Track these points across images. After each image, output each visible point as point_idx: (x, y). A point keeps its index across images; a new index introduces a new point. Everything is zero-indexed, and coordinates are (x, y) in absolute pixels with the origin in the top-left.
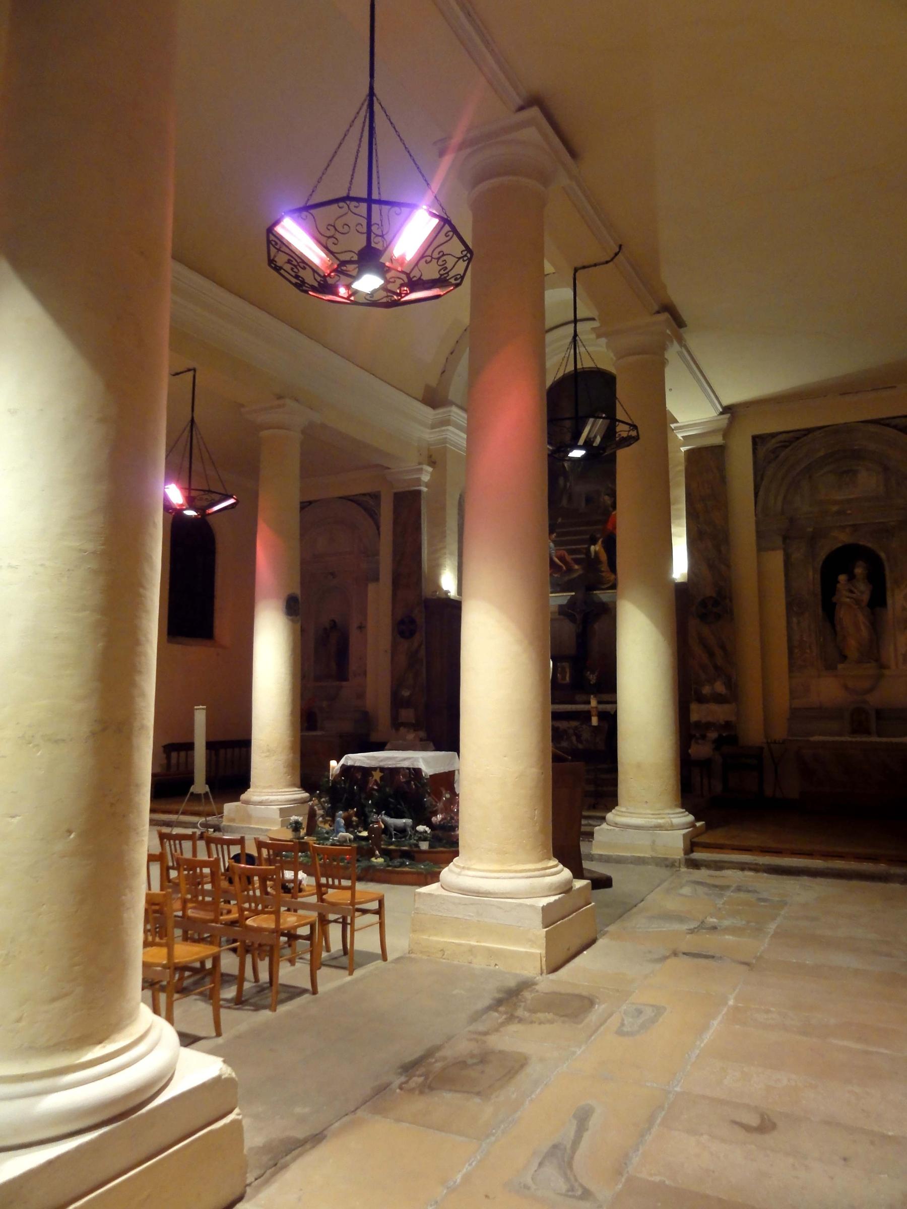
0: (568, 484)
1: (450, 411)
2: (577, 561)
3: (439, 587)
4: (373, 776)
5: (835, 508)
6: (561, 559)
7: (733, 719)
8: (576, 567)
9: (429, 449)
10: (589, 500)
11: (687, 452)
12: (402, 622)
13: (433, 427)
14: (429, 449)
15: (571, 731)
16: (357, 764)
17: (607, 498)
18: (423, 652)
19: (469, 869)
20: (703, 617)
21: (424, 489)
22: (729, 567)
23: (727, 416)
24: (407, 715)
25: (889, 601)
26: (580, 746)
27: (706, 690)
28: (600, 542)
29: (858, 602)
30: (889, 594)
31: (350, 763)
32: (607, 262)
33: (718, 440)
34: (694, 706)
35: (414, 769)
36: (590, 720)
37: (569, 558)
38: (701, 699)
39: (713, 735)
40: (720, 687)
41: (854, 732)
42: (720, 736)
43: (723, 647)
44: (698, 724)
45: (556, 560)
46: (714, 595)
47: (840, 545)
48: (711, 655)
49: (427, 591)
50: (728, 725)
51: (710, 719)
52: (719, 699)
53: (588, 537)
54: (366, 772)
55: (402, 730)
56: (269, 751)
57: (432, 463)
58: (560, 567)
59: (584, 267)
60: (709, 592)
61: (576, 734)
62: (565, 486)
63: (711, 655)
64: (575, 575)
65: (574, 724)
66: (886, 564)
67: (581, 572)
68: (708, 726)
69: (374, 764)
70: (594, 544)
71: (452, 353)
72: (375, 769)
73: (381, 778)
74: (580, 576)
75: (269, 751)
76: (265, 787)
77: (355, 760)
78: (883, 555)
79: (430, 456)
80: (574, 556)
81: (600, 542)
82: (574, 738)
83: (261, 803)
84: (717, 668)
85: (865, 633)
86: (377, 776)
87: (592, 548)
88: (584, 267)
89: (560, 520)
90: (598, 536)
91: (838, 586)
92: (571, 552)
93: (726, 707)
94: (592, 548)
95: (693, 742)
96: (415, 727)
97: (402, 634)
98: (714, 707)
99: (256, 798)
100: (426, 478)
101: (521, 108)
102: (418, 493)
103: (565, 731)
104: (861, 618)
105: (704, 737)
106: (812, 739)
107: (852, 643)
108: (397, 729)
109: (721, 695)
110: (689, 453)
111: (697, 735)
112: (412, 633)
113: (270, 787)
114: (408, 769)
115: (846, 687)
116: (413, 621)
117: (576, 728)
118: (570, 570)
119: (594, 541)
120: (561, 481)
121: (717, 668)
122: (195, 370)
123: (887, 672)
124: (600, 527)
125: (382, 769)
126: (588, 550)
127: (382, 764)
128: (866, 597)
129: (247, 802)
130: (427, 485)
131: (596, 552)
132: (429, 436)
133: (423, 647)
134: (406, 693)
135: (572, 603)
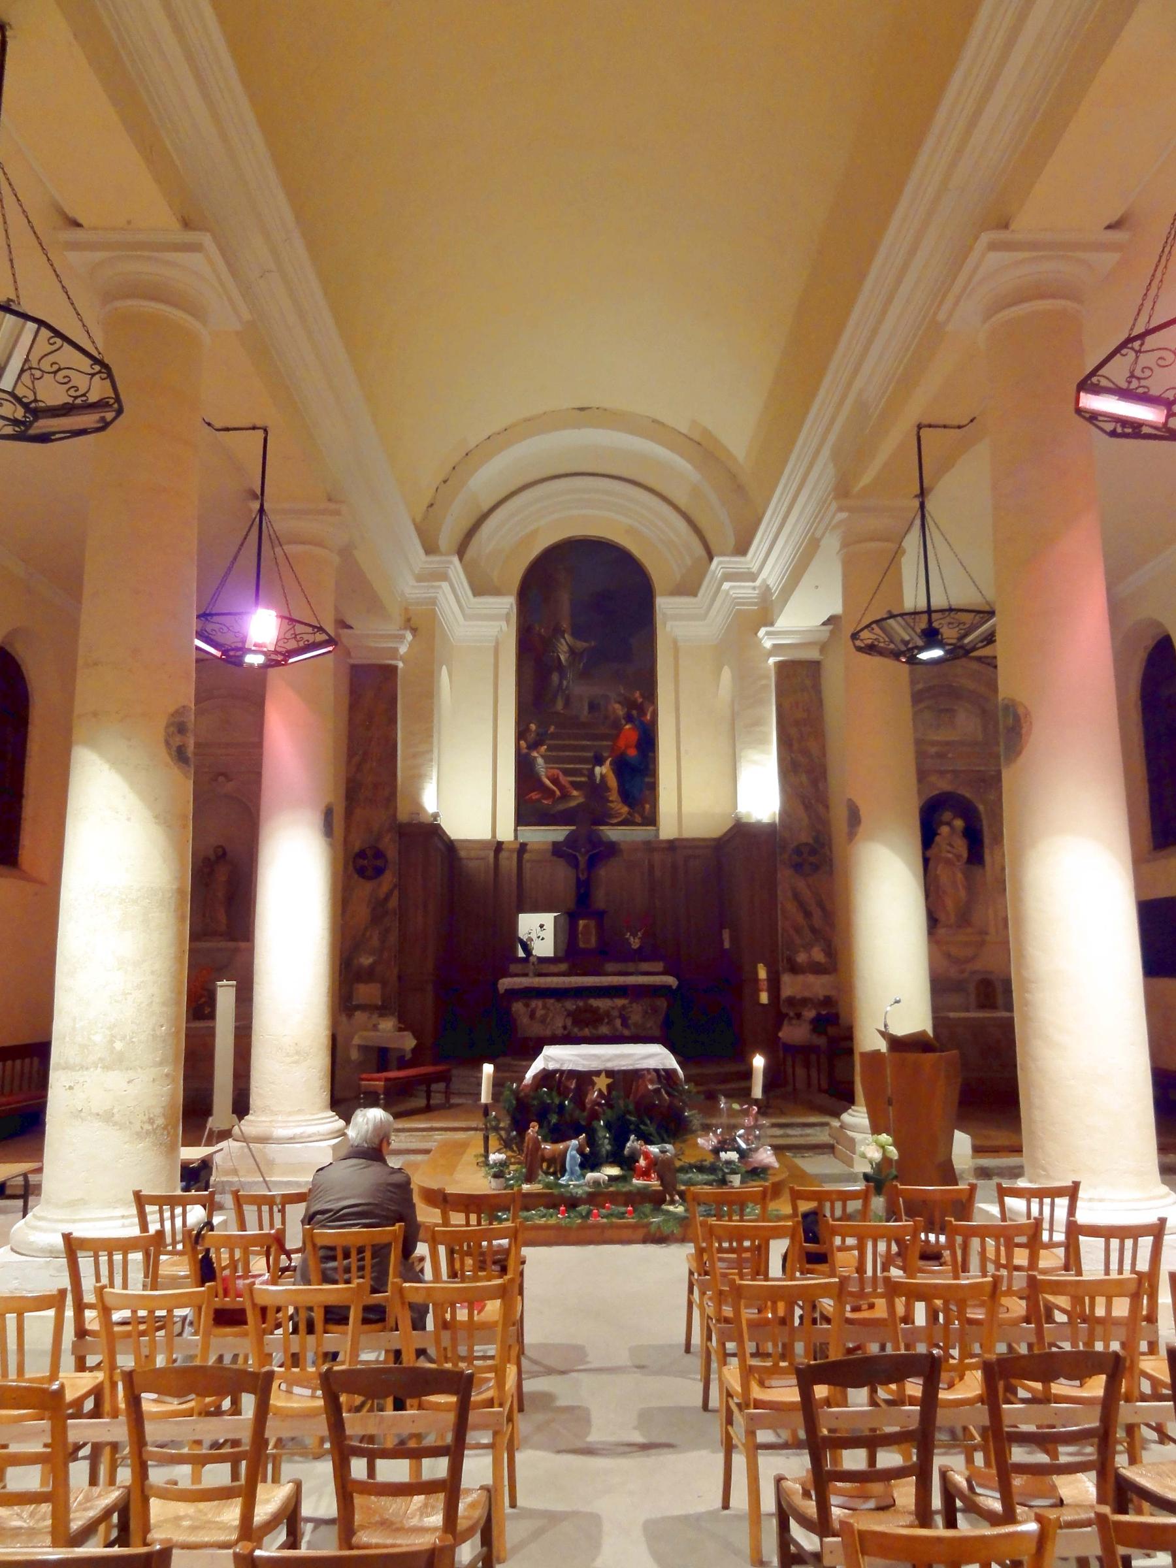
0: (565, 683)
1: (451, 562)
2: (575, 785)
3: (418, 807)
4: (593, 1084)
5: (933, 750)
6: (555, 781)
7: (833, 993)
8: (575, 793)
9: (406, 609)
10: (593, 707)
11: (776, 663)
12: (362, 854)
13: (420, 578)
14: (406, 609)
15: (615, 1013)
16: (567, 1067)
17: (617, 706)
18: (393, 903)
19: (1101, 1200)
20: (798, 867)
21: (401, 665)
22: (827, 807)
23: (830, 627)
24: (368, 992)
25: (987, 858)
27: (801, 958)
28: (608, 762)
29: (959, 857)
30: (987, 852)
31: (551, 1066)
32: (959, 427)
33: (813, 654)
34: (786, 978)
35: (666, 1071)
36: (758, 996)
37: (564, 780)
38: (795, 969)
39: (810, 1014)
40: (818, 955)
41: (982, 1006)
42: (819, 1015)
43: (821, 905)
44: (791, 1001)
45: (547, 782)
46: (811, 841)
47: (937, 792)
48: (808, 915)
49: (403, 815)
50: (828, 1001)
51: (807, 994)
52: (818, 969)
53: (591, 754)
54: (584, 1078)
55: (358, 1015)
56: (298, 1053)
57: (414, 631)
58: (554, 792)
59: (930, 426)
60: (805, 837)
62: (561, 683)
63: (808, 915)
64: (573, 804)
65: (620, 1002)
66: (983, 816)
67: (581, 800)
68: (805, 1002)
69: (594, 1065)
70: (601, 765)
71: (445, 482)
72: (598, 1073)
73: (609, 1086)
74: (579, 805)
75: (298, 1053)
76: (290, 1114)
77: (563, 1062)
78: (981, 808)
79: (409, 620)
80: (571, 779)
81: (608, 762)
82: (618, 1022)
83: (291, 1140)
84: (813, 930)
85: (963, 894)
86: (602, 1083)
87: (598, 770)
88: (930, 426)
89: (552, 729)
90: (605, 754)
91: (937, 839)
92: (566, 772)
93: (825, 979)
94: (598, 770)
95: (786, 1022)
96: (382, 1010)
97: (361, 872)
98: (811, 978)
99: (281, 1132)
100: (403, 650)
101: (1109, 227)
102: (393, 670)
103: (607, 1014)
104: (960, 876)
105: (799, 1016)
106: (952, 1015)
107: (949, 903)
108: (350, 1016)
109: (819, 963)
110: (780, 666)
111: (792, 1014)
112: (379, 872)
113: (300, 1111)
114: (657, 1071)
115: (948, 956)
116: (379, 854)
117: (624, 1007)
118: (565, 796)
119: (599, 761)
120: (555, 677)
121: (813, 930)
122: (265, 431)
123: (988, 938)
124: (610, 743)
125: (610, 1073)
126: (592, 771)
127: (610, 1065)
128: (965, 855)
129: (264, 1140)
130: (402, 659)
131: (603, 776)
132: (409, 589)
133: (396, 893)
134: (366, 961)
135: (571, 840)
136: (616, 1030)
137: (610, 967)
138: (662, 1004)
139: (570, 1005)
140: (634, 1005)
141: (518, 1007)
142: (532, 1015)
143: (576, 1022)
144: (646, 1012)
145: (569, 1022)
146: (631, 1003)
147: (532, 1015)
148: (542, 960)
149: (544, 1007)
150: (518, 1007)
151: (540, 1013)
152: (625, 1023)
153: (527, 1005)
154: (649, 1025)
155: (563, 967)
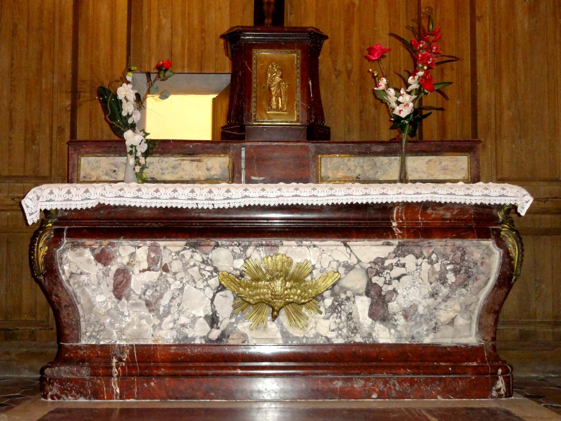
15: (356, 281)
26: (384, 336)
61: (372, 290)
65: (368, 250)
82: (362, 305)
136: (355, 330)
137: (330, 164)
138: (487, 256)
139: (226, 256)
140: (410, 260)
141: (78, 264)
142: (120, 288)
143: (242, 305)
144: (443, 280)
145: (225, 305)
146: (400, 252)
147: (120, 288)
148: (159, 148)
149: (152, 264)
150: (78, 264)
151: (138, 281)
152: (380, 309)
153: (103, 258)
154: (444, 316)
155: (218, 163)
